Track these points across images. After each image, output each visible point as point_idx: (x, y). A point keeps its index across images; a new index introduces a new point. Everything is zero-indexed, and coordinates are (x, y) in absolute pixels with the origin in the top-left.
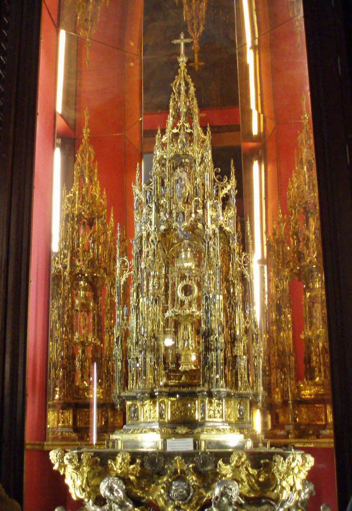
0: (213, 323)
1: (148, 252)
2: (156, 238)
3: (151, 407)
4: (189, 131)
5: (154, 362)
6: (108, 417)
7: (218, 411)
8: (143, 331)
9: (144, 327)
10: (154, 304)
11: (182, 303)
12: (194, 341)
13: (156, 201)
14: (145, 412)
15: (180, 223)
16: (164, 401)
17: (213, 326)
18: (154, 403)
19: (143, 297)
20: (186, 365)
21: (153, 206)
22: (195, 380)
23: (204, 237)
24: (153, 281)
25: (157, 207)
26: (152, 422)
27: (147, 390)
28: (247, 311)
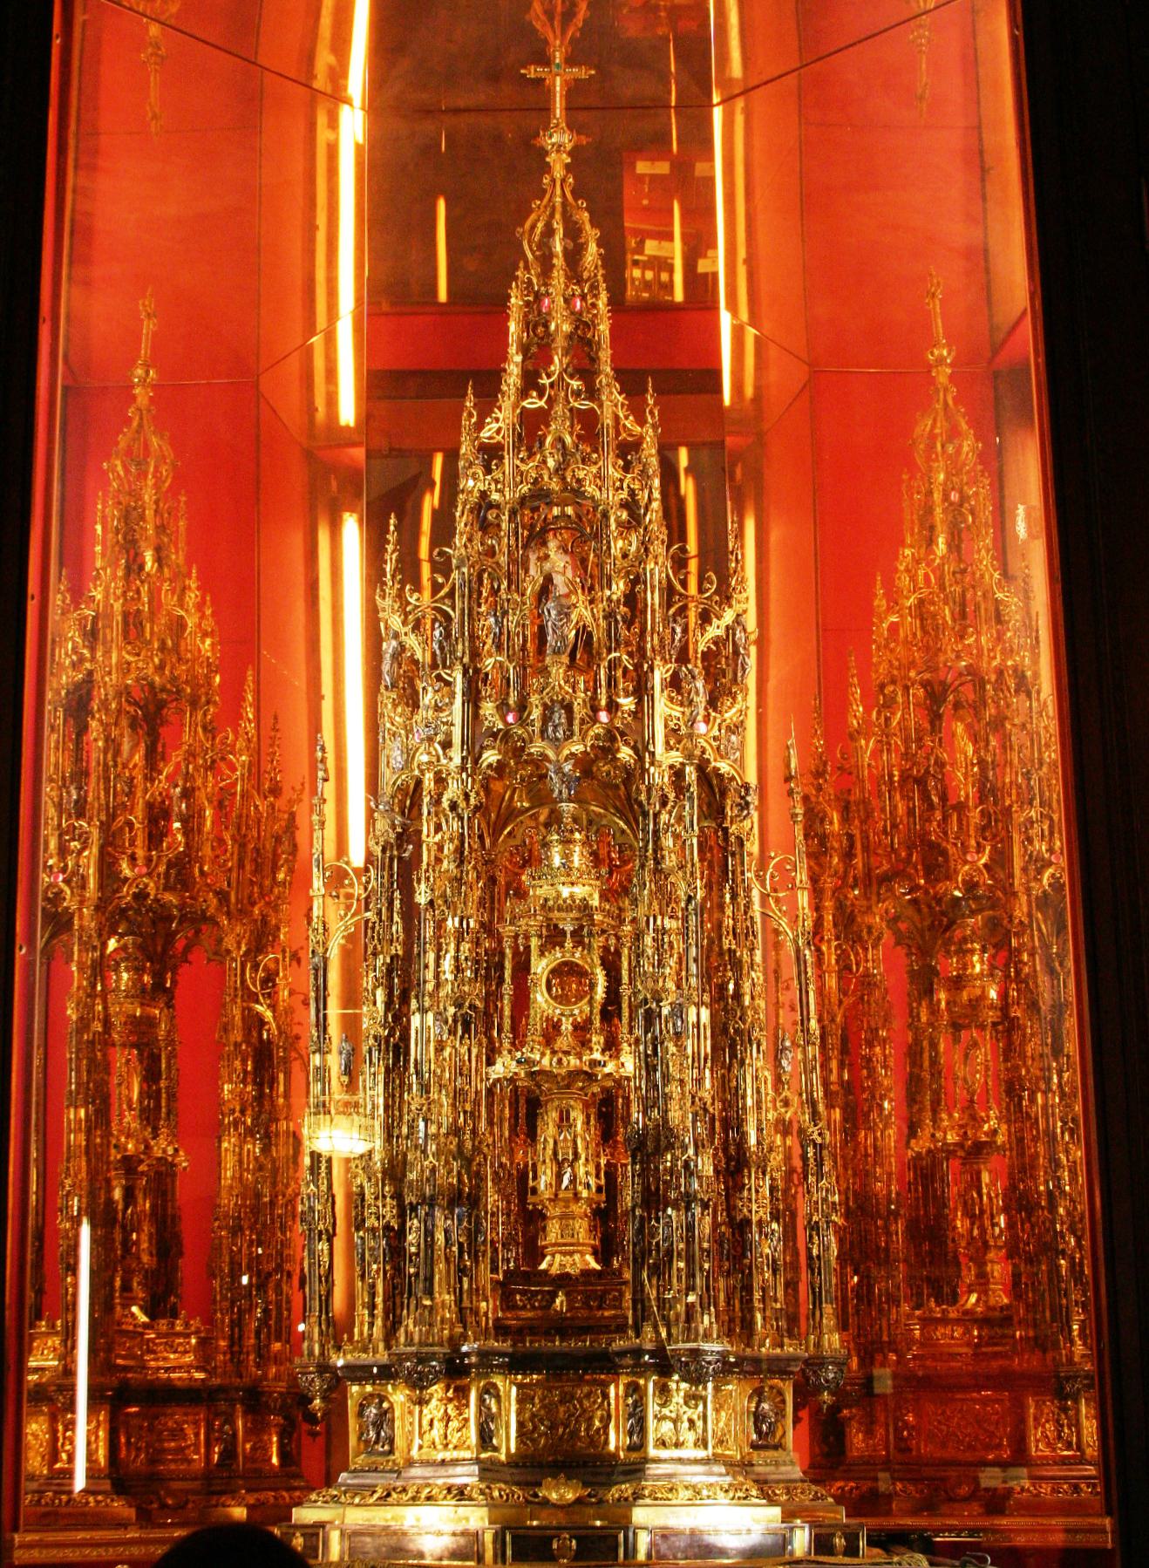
0: (674, 1106)
1: (440, 848)
2: (467, 796)
3: (450, 1407)
4: (585, 405)
5: (461, 1245)
6: (235, 1435)
7: (691, 1421)
8: (422, 1135)
9: (426, 1120)
10: (460, 1032)
11: (551, 1031)
12: (591, 1168)
13: (466, 660)
14: (425, 1423)
15: (557, 744)
16: (494, 1386)
17: (675, 1115)
18: (462, 1393)
20: (564, 1254)
21: (458, 677)
22: (600, 1308)
23: (643, 797)
24: (458, 950)
25: (469, 682)
26: (455, 1462)
27: (436, 1349)
28: (784, 1063)
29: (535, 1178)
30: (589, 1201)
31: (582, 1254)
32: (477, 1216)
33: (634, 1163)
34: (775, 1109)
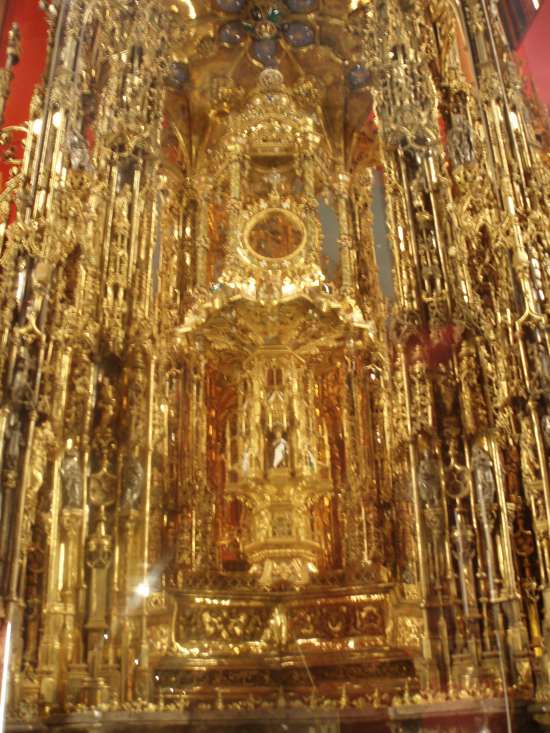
5: (95, 509)
20: (278, 559)
29: (235, 458)
31: (305, 561)
32: (127, 459)
33: (410, 363)
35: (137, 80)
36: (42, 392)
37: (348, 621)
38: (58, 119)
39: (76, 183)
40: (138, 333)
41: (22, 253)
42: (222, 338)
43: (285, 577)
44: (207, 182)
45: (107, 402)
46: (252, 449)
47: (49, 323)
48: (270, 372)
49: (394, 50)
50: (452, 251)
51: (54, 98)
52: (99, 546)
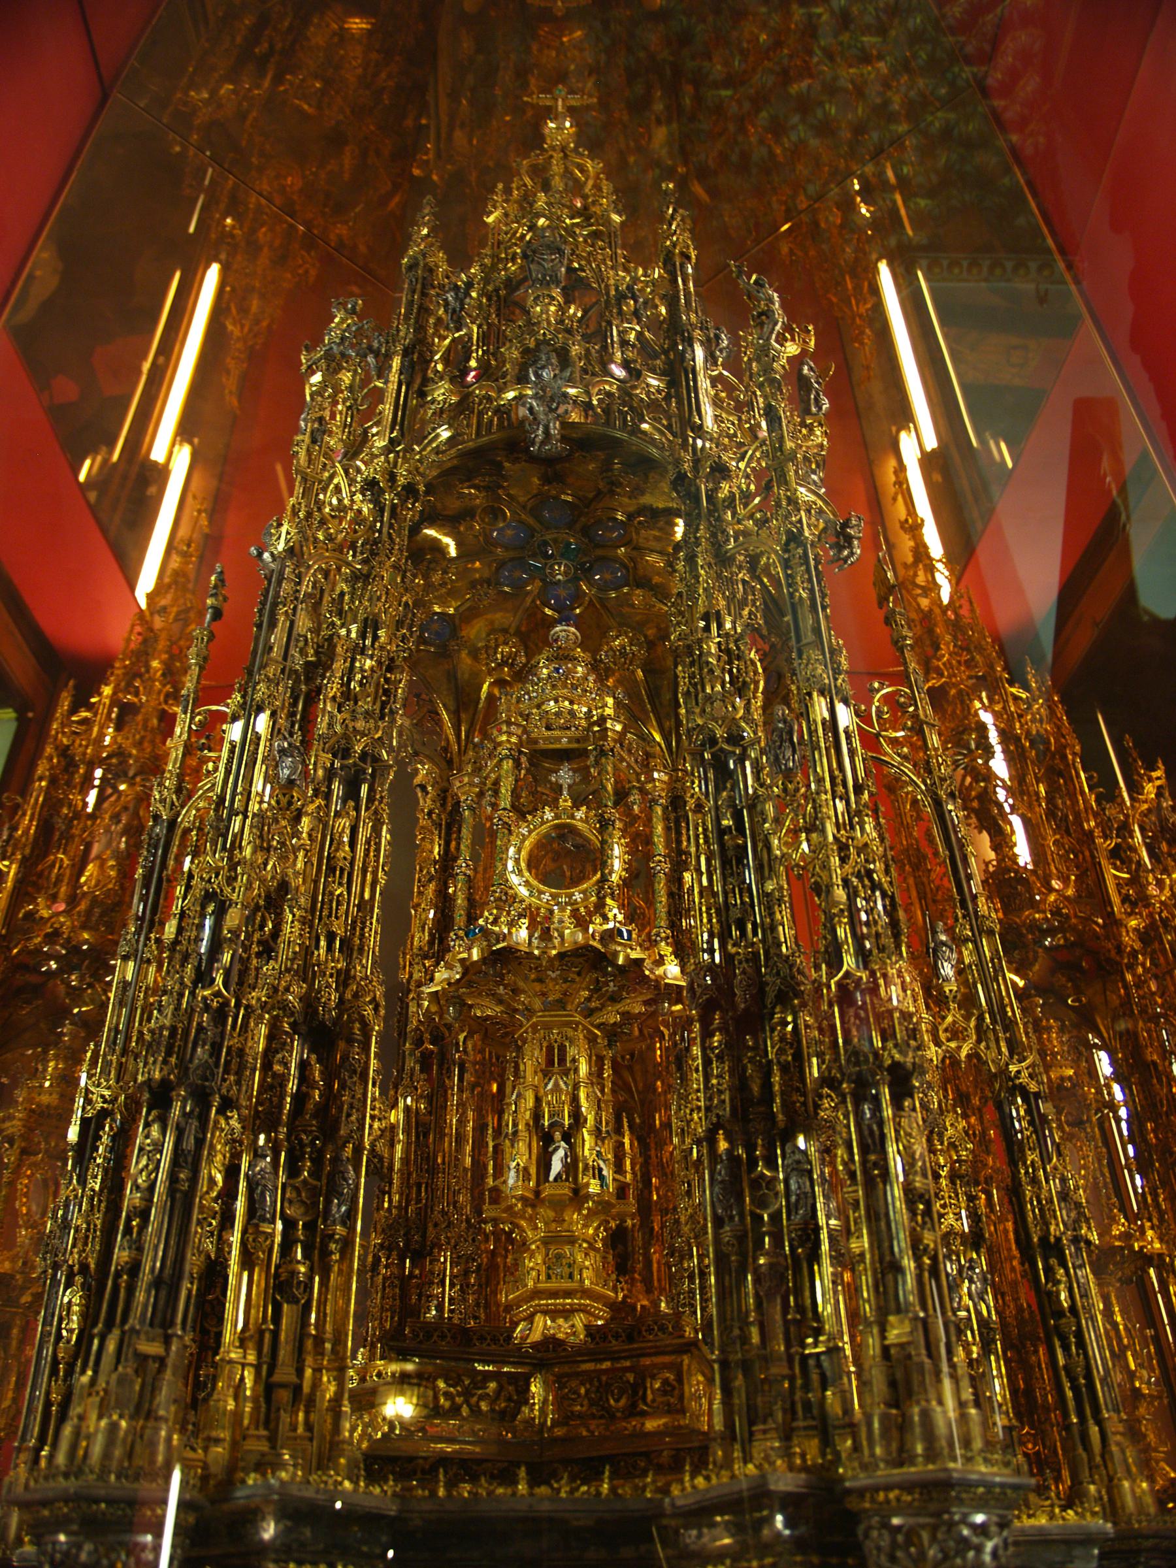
5: (289, 1224)
19: (250, 709)
20: (554, 1314)
22: (632, 1411)
29: (500, 1171)
30: (603, 1207)
32: (336, 1160)
33: (707, 1034)
34: (938, 1043)
35: (368, 663)
36: (227, 1071)
37: (635, 1393)
38: (262, 723)
39: (284, 801)
40: (356, 995)
41: (209, 897)
42: (486, 1002)
43: (561, 1336)
44: (471, 784)
45: (313, 1085)
46: (521, 1155)
47: (241, 983)
48: (550, 1049)
49: (706, 617)
50: (770, 887)
51: (258, 696)
52: (294, 1273)
